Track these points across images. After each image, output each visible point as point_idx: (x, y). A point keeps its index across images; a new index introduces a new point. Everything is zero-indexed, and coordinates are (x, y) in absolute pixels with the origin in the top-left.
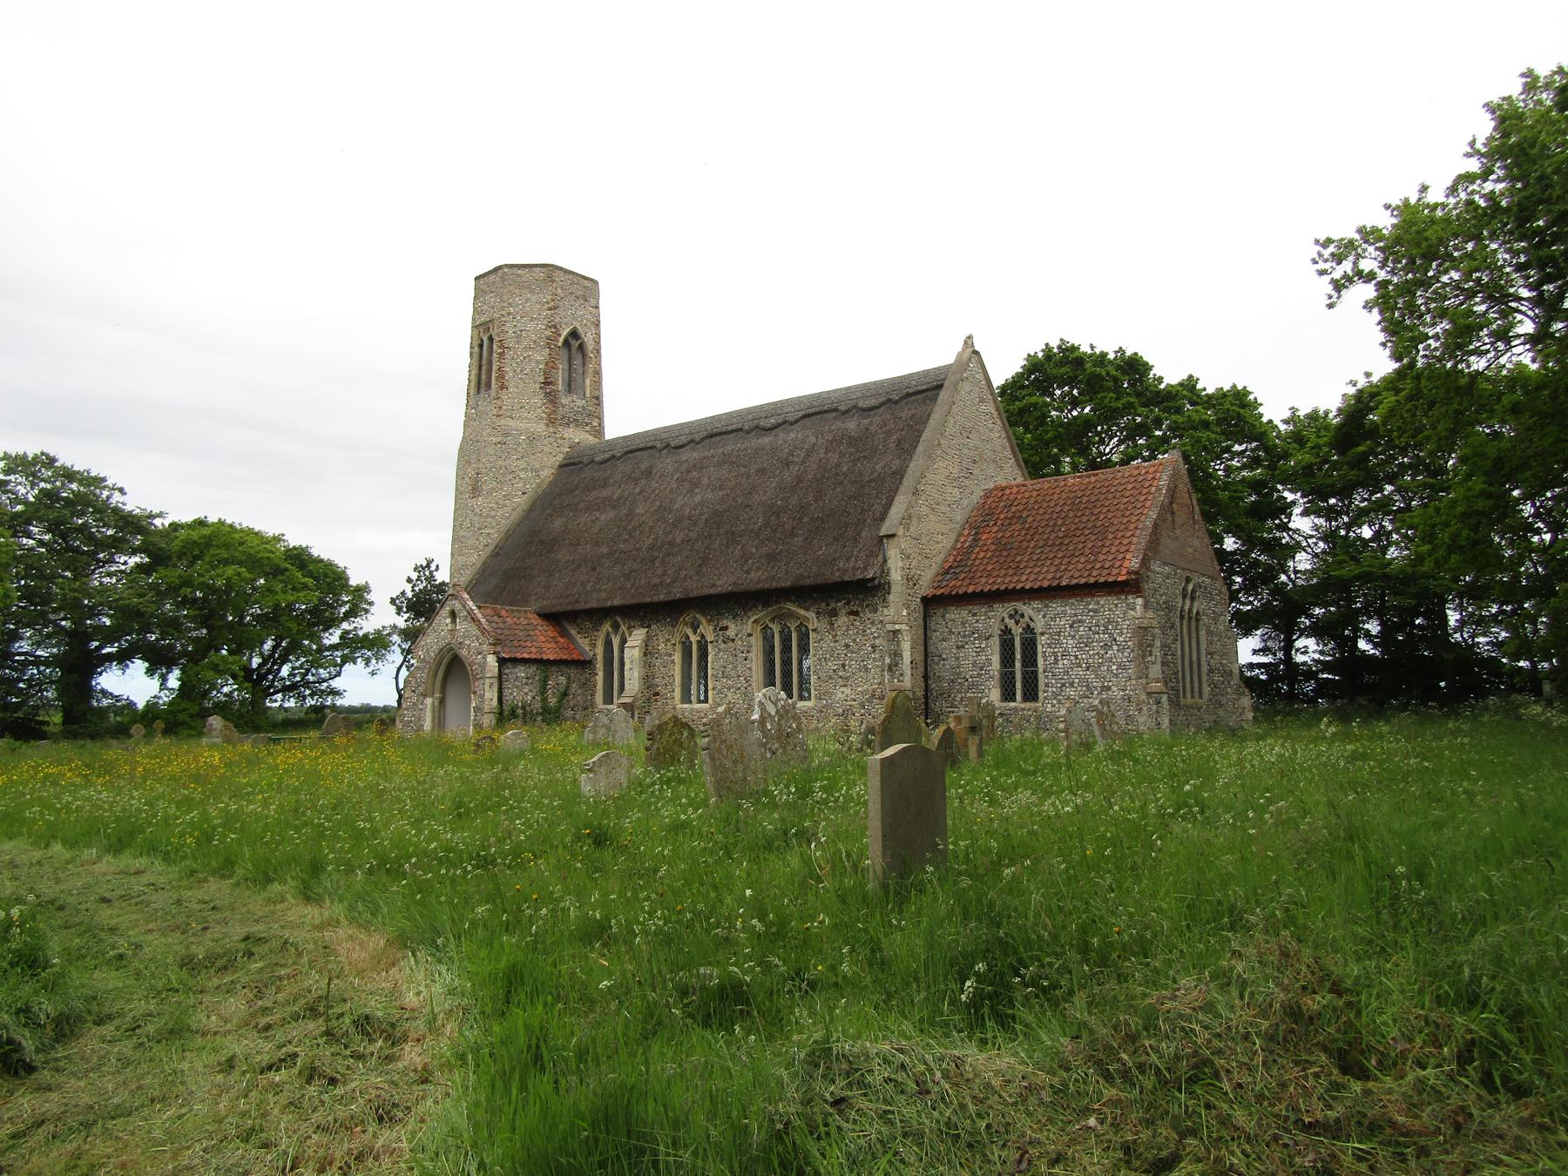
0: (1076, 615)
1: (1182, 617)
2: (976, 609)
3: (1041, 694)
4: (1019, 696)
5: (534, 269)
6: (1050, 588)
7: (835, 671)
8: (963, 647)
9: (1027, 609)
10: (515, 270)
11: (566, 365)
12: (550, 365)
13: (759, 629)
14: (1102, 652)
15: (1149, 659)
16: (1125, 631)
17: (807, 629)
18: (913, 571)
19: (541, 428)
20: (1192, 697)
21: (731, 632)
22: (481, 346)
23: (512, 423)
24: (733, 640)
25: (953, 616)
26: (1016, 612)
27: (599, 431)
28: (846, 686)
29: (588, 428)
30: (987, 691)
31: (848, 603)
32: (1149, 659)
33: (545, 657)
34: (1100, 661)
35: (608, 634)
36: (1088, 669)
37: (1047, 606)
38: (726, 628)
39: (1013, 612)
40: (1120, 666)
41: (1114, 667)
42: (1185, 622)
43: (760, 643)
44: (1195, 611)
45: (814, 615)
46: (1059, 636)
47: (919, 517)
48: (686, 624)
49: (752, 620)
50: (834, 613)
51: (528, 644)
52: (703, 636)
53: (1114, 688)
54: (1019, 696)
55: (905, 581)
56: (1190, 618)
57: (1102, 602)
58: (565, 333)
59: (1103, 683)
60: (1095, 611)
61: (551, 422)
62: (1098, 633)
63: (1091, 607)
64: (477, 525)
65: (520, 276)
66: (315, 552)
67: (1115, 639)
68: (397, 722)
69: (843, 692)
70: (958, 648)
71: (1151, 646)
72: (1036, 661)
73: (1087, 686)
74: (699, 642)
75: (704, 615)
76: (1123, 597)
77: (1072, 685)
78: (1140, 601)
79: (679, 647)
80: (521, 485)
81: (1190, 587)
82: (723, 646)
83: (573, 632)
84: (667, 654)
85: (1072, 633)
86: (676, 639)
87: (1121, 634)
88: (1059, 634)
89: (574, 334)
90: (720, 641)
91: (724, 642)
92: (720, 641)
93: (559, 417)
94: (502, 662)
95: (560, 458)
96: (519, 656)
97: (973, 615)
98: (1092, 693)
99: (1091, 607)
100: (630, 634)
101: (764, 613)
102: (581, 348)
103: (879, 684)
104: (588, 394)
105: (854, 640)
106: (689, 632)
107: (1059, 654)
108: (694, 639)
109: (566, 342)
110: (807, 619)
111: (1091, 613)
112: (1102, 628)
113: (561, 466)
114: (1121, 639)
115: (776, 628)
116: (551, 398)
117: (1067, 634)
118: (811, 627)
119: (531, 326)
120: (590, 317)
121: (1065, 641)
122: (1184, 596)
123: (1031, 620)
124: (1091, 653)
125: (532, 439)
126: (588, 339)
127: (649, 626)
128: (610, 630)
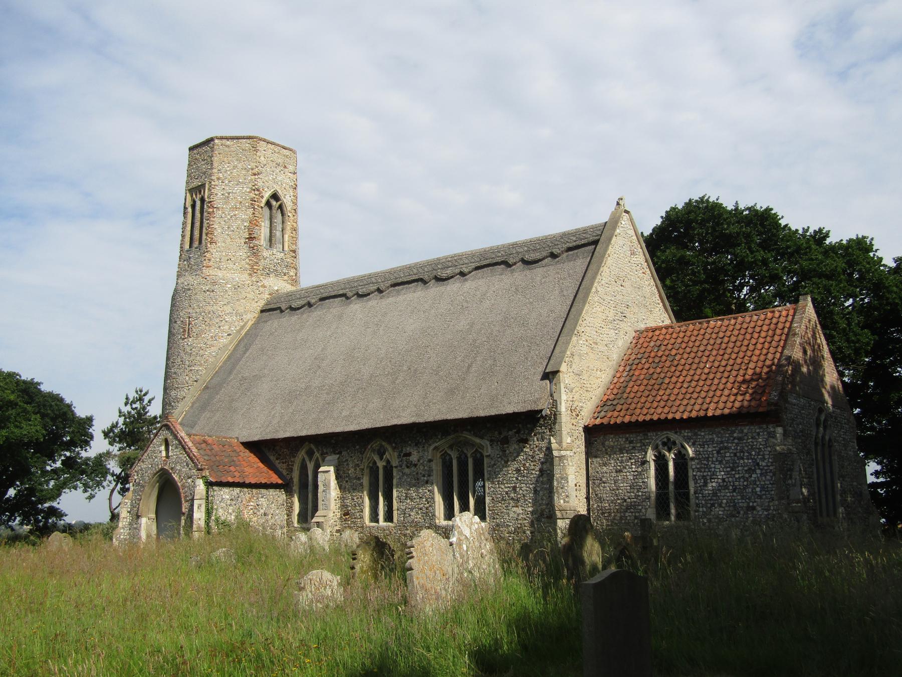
0: (722, 442)
1: (816, 444)
2: (632, 437)
4: (673, 518)
5: (240, 141)
6: (698, 419)
7: (507, 493)
8: (620, 471)
10: (224, 141)
11: (268, 223)
12: (254, 223)
13: (439, 455)
14: (747, 475)
15: (790, 482)
16: (767, 457)
17: (482, 455)
18: (576, 404)
19: (245, 276)
20: (828, 515)
21: (414, 458)
22: (193, 206)
23: (220, 274)
25: (612, 444)
26: (669, 439)
27: (295, 281)
28: (517, 507)
29: (286, 278)
30: (643, 510)
31: (518, 432)
32: (790, 482)
33: (247, 482)
34: (745, 483)
35: (304, 460)
36: (734, 490)
37: (696, 434)
38: (409, 454)
39: (665, 440)
40: (763, 488)
41: (758, 489)
42: (819, 448)
43: (440, 468)
44: (827, 438)
45: (488, 443)
46: (708, 461)
47: (580, 355)
48: (373, 451)
49: (432, 447)
50: (506, 441)
51: (232, 468)
52: (388, 462)
53: (759, 508)
54: (673, 518)
55: (569, 412)
56: (823, 445)
57: (745, 431)
58: (267, 195)
59: (749, 503)
60: (740, 439)
61: (253, 271)
62: (743, 459)
63: (735, 435)
65: (228, 146)
66: (45, 388)
67: (758, 464)
68: (114, 540)
70: (616, 472)
71: (791, 470)
72: (687, 483)
73: (734, 506)
74: (385, 467)
75: (390, 443)
76: (765, 426)
77: (720, 505)
78: (780, 430)
79: (367, 471)
80: (227, 327)
81: (823, 418)
82: (407, 471)
83: (272, 458)
85: (719, 459)
86: (365, 464)
87: (763, 459)
88: (707, 459)
89: (275, 196)
90: (404, 466)
91: (408, 467)
92: (404, 466)
93: (261, 268)
94: (209, 484)
95: (261, 304)
96: (224, 480)
97: (631, 442)
98: (739, 513)
99: (735, 435)
100: (323, 460)
101: (444, 441)
102: (280, 207)
103: (547, 505)
104: (286, 248)
105: (524, 465)
106: (376, 458)
107: (708, 478)
108: (381, 464)
109: (268, 204)
110: (482, 447)
111: (736, 441)
112: (746, 454)
113: (262, 311)
114: (764, 464)
115: (454, 455)
116: (254, 251)
117: (714, 459)
118: (485, 454)
119: (237, 189)
120: (288, 181)
121: (713, 466)
122: (818, 426)
124: (737, 476)
125: (236, 288)
126: (287, 200)
127: (340, 453)
128: (306, 457)
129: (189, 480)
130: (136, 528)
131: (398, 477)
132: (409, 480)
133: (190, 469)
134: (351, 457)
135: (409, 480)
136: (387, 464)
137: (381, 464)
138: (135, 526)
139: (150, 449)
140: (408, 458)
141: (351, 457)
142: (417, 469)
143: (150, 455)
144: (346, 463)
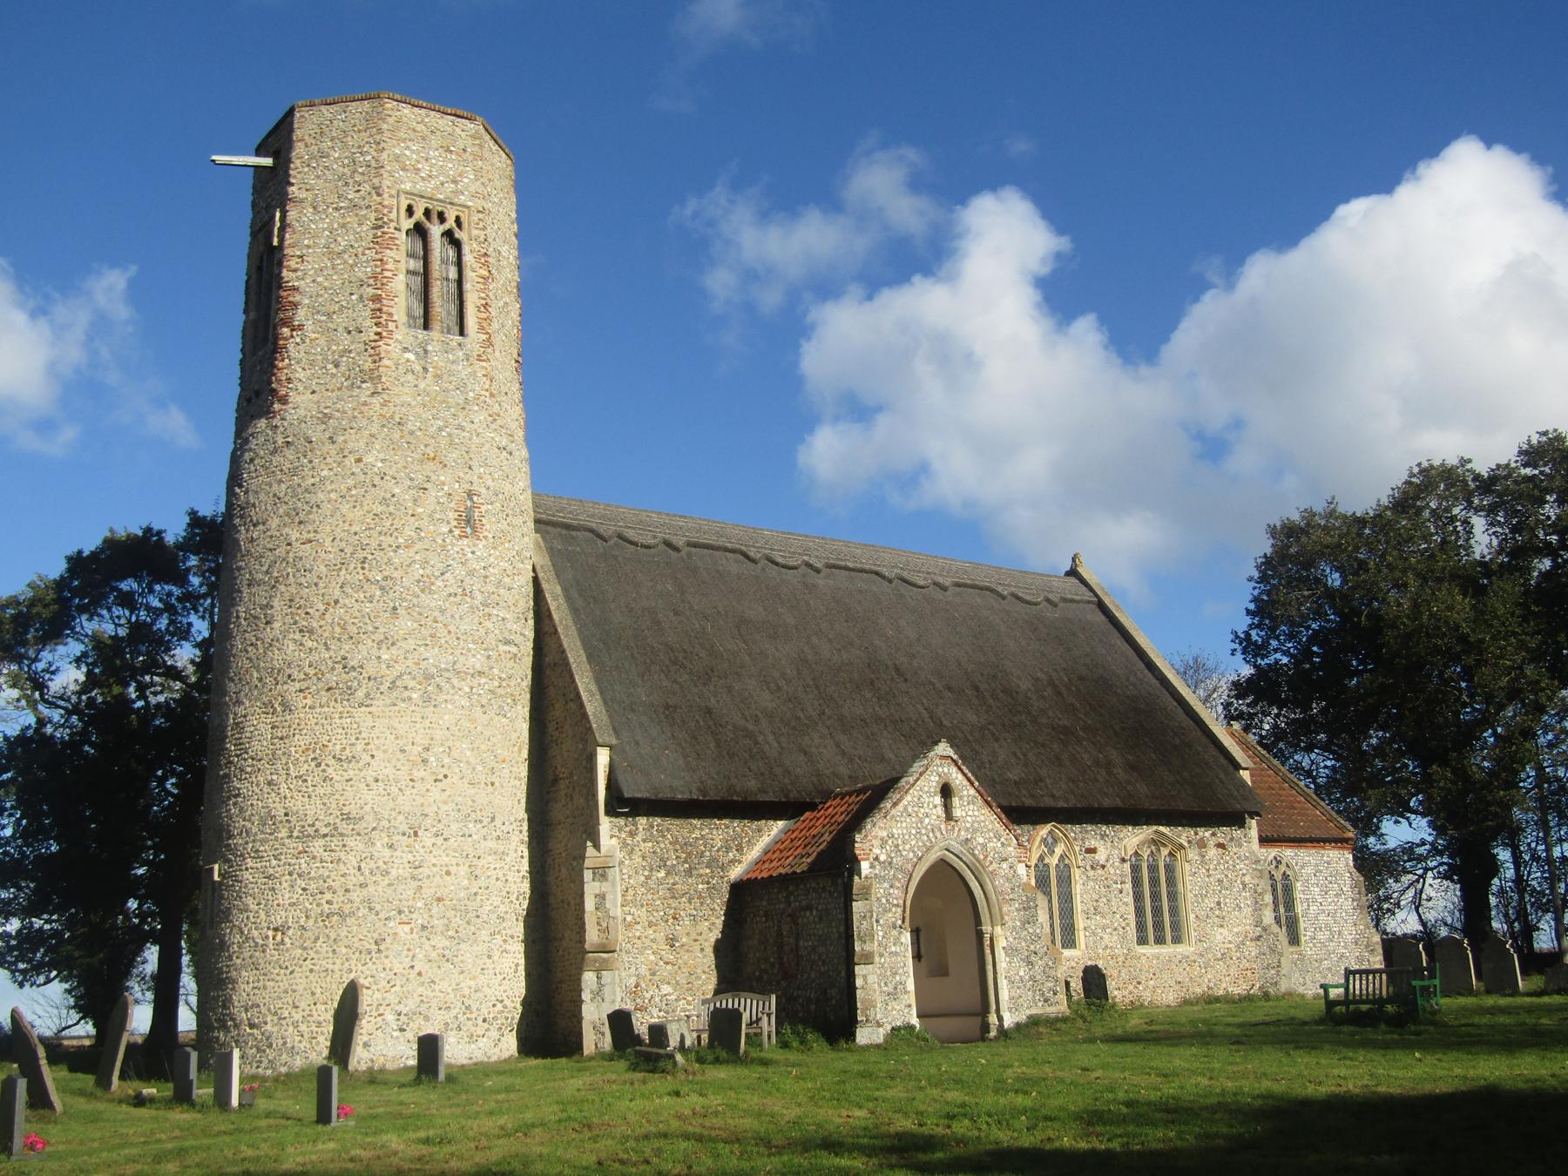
3: (1303, 939)
9: (1288, 853)
21: (1101, 856)
24: (1103, 867)
28: (1222, 926)
31: (1214, 834)
60: (1328, 863)
64: (480, 597)
69: (1221, 933)
82: (1091, 873)
123: (1288, 866)
129: (1005, 865)
130: (896, 954)
133: (1003, 844)
137: (1053, 861)
138: (893, 949)
139: (909, 798)
143: (910, 809)
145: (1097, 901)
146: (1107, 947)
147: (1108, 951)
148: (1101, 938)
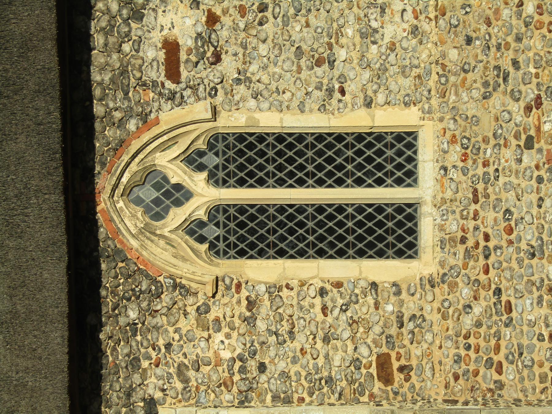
84: (250, 321)
91: (217, 59)
131: (252, 103)
132: (263, 49)
134: (168, 346)
135: (263, 49)
136: (201, 168)
140: (183, 56)
141: (168, 346)
142: (225, 12)
144: (191, 374)
145: (299, 53)
146: (415, 31)
147: (426, 26)
148: (392, 47)
